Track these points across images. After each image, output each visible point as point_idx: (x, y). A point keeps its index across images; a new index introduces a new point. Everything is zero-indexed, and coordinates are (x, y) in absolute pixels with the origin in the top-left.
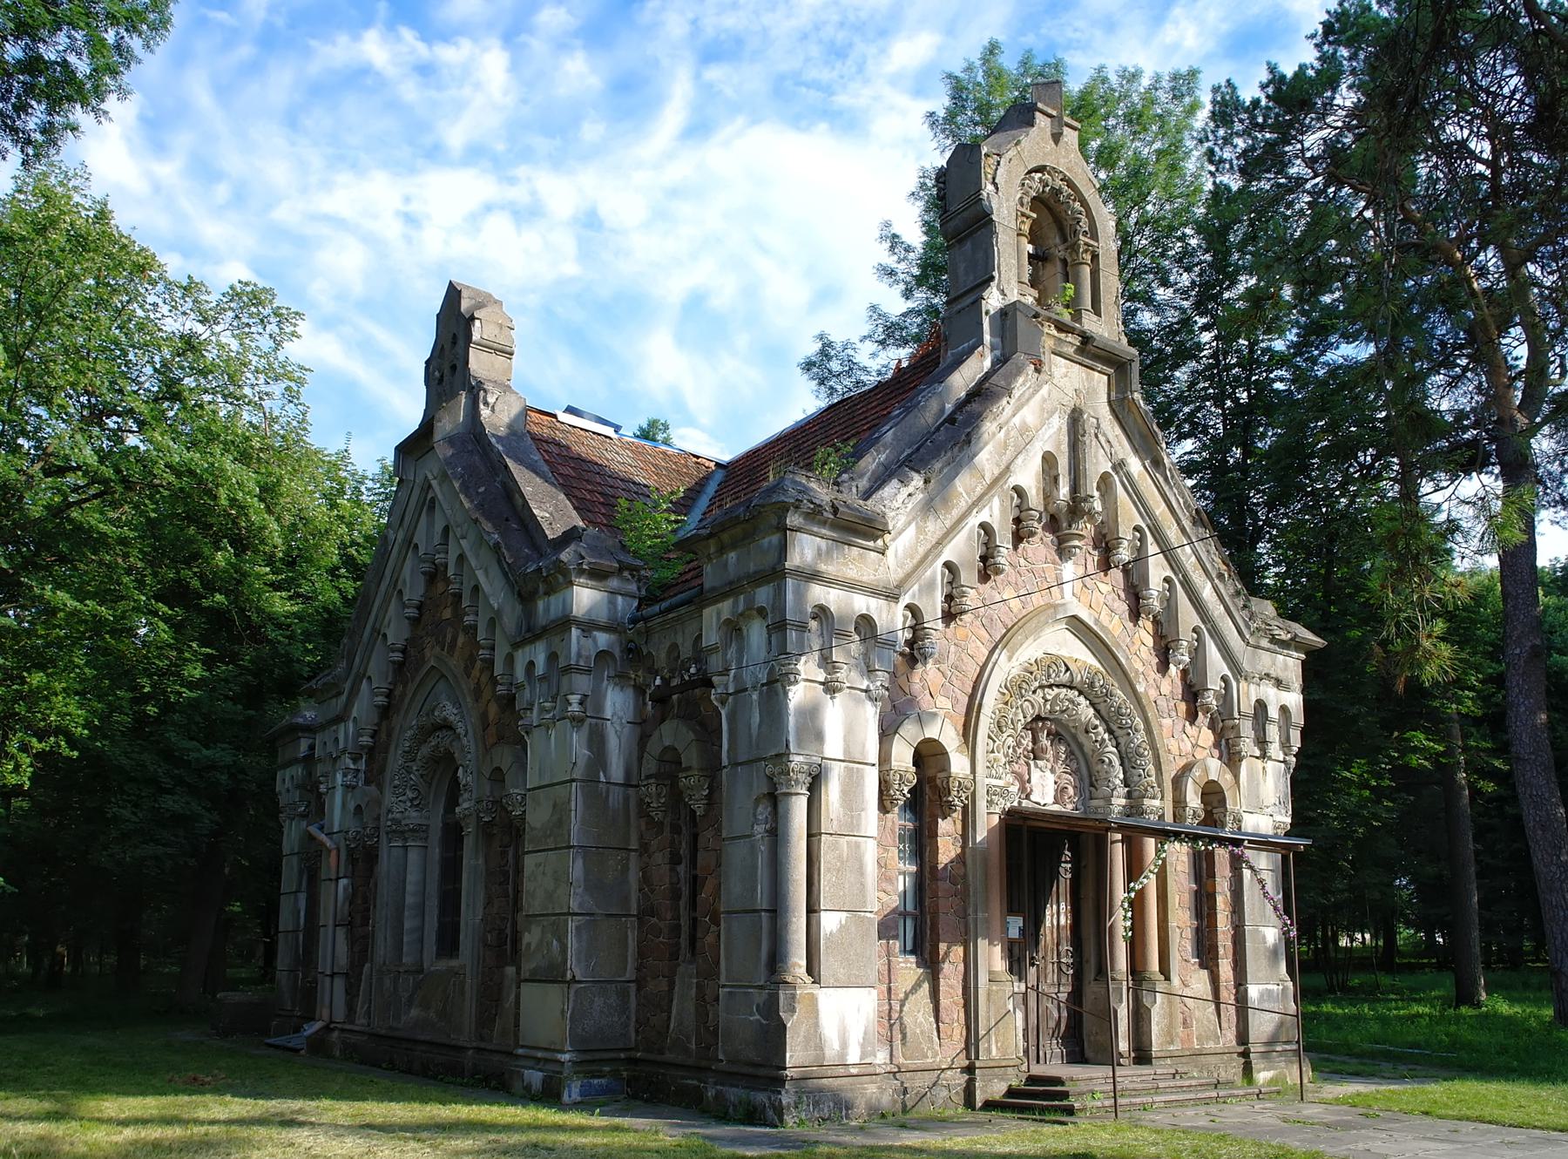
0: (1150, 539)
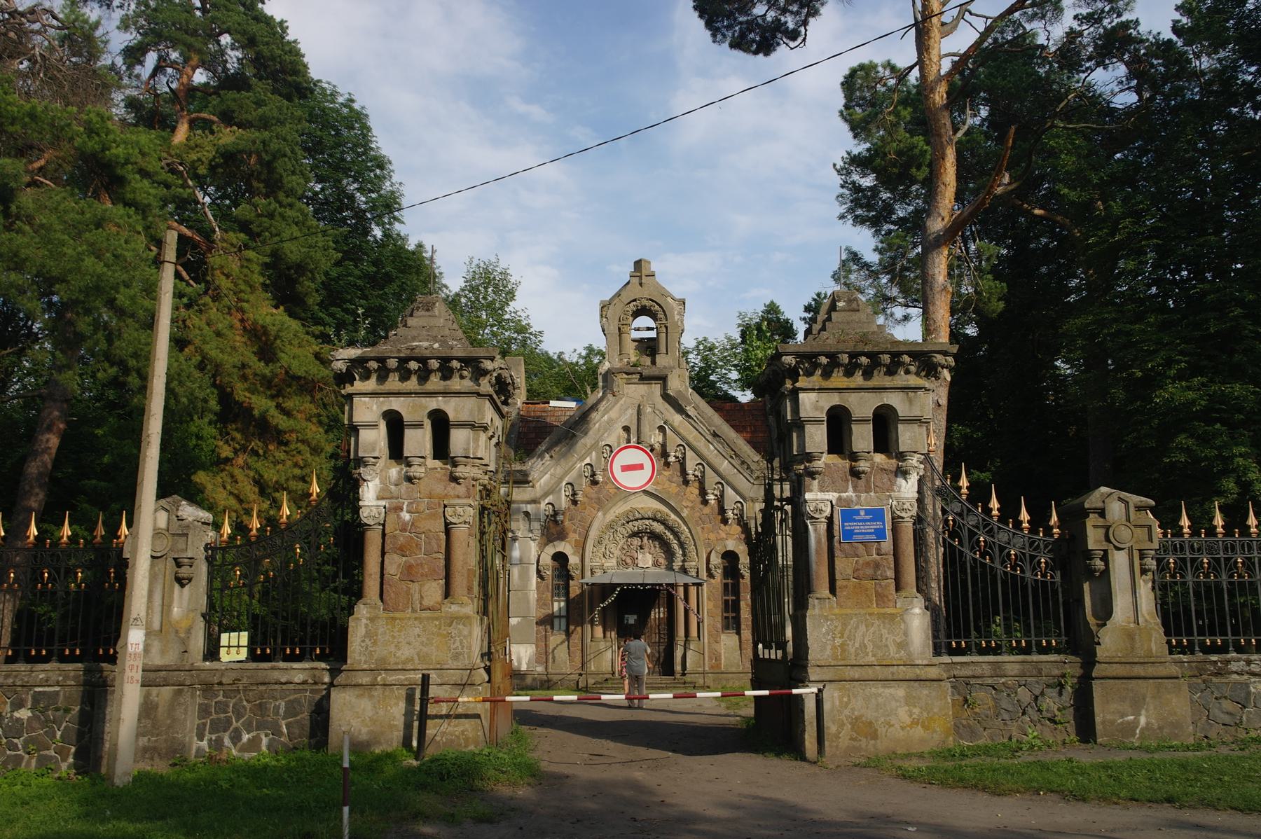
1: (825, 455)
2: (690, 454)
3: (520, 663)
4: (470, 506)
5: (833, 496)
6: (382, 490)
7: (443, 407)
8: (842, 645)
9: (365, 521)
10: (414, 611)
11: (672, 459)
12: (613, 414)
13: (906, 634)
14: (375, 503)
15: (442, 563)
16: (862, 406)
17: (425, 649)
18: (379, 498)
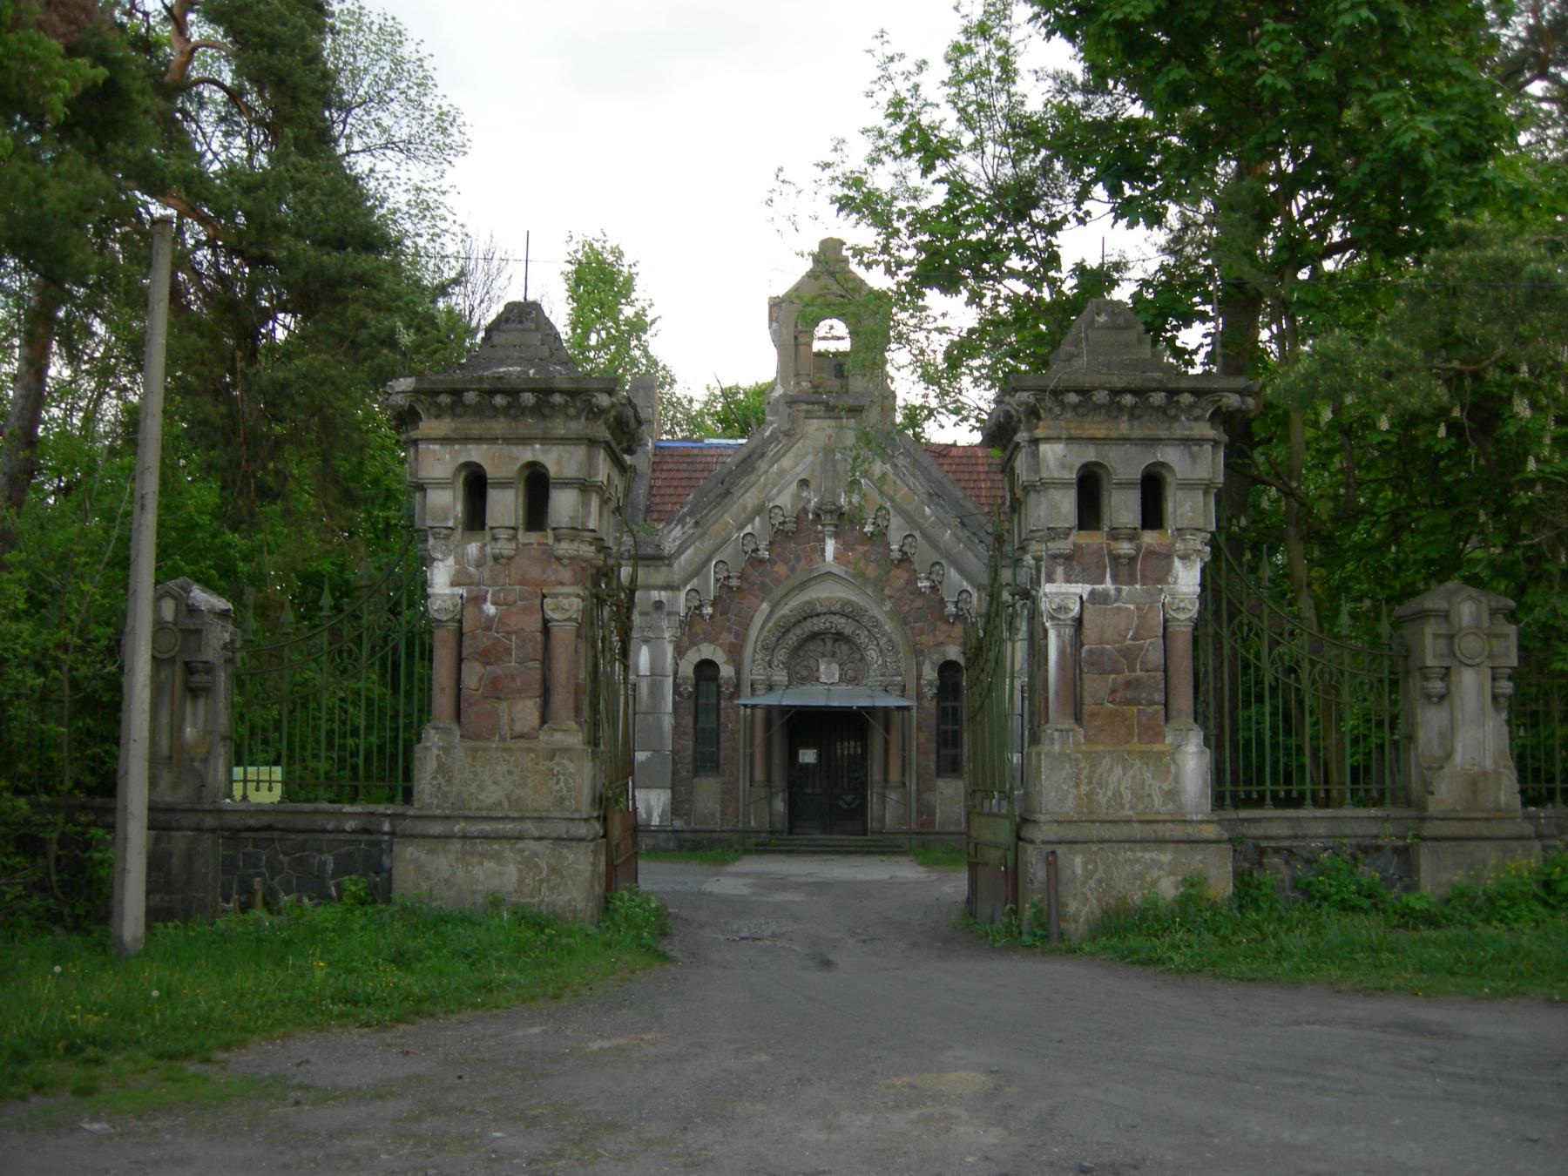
1: (1074, 532)
3: (650, 815)
4: (578, 596)
5: (1083, 589)
6: (458, 573)
7: (541, 458)
8: (1090, 794)
9: (436, 615)
10: (503, 739)
12: (786, 462)
13: (1177, 779)
14: (448, 591)
15: (537, 676)
16: (1127, 465)
17: (518, 791)
18: (453, 584)
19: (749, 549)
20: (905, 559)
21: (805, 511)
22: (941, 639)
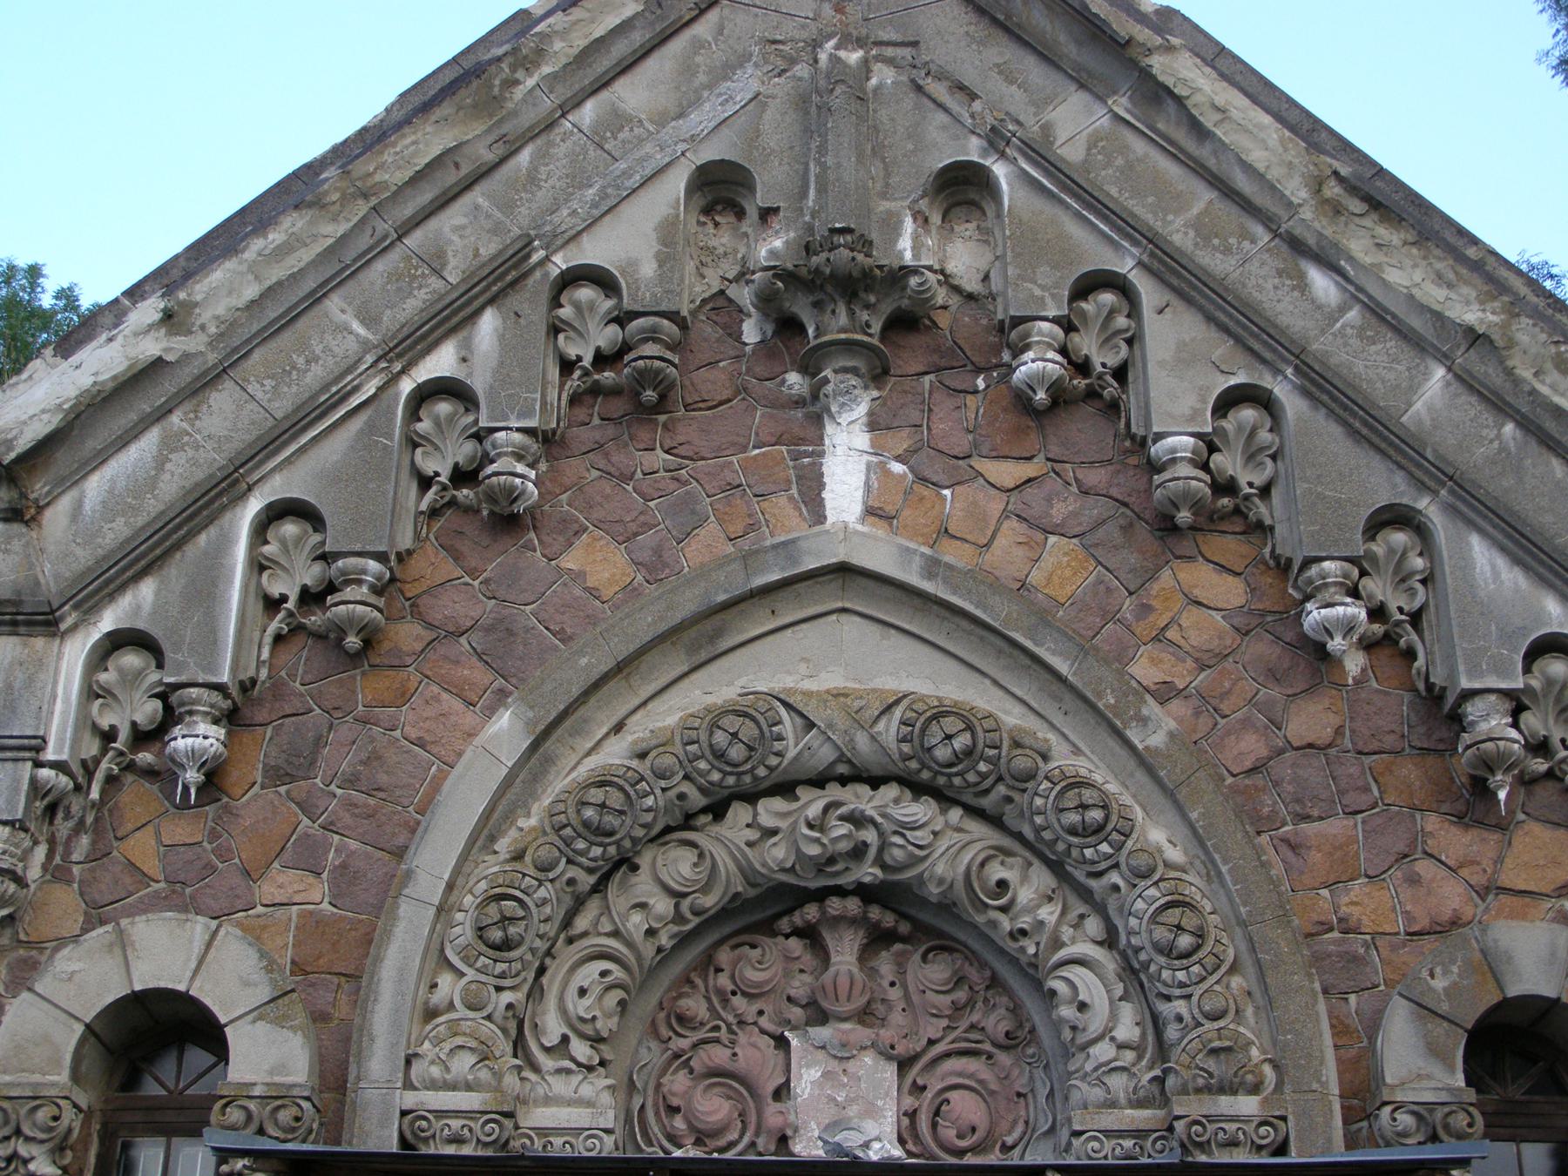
0: (1148, 292)
2: (1168, 331)
11: (1038, 365)
19: (438, 466)
20: (1227, 511)
21: (721, 306)
22: (1451, 896)
